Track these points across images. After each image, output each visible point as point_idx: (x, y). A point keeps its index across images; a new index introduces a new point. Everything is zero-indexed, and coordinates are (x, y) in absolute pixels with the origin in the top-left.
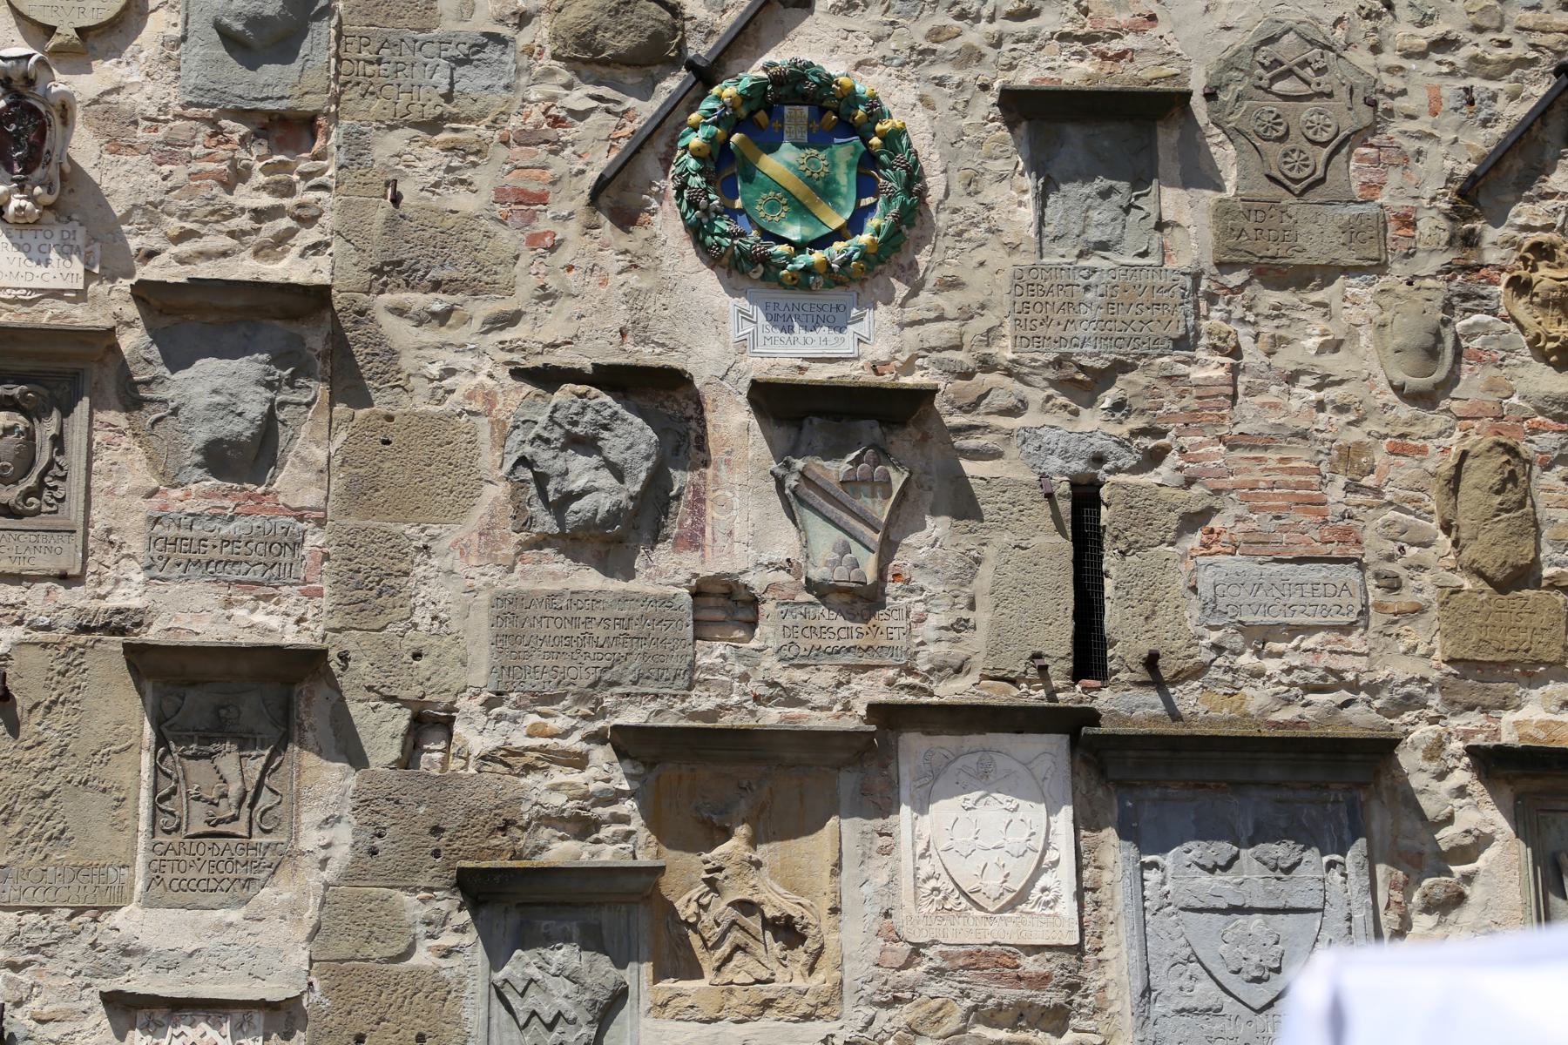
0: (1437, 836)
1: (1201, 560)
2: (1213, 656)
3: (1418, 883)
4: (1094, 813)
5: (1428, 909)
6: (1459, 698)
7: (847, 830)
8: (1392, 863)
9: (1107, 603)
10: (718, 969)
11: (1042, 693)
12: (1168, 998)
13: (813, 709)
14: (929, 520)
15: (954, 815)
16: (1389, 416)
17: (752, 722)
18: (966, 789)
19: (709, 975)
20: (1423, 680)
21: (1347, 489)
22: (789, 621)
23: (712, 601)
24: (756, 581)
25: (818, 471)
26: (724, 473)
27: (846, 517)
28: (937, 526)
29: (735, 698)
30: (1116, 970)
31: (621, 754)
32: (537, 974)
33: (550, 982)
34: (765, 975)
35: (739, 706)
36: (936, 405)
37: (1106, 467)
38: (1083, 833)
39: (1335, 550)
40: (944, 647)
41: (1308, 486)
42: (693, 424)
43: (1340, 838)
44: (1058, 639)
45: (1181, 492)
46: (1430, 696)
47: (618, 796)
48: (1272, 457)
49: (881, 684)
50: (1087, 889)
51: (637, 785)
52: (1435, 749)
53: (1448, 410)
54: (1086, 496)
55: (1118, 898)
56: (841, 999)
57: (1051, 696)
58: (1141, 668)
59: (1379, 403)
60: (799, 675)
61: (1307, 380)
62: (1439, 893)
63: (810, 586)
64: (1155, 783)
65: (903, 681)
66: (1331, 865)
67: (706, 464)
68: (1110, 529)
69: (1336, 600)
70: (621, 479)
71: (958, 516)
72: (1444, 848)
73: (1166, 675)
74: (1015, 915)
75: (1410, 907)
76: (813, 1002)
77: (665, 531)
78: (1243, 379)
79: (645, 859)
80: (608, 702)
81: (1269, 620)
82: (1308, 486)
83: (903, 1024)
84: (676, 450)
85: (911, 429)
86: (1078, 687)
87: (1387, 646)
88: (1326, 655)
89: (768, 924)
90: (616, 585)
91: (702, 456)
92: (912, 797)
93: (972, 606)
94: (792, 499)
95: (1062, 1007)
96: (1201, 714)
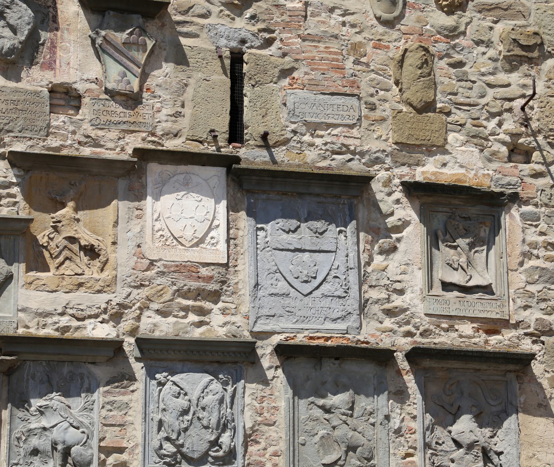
0: (386, 221)
1: (288, 91)
2: (292, 135)
3: (377, 241)
4: (236, 204)
5: (381, 253)
6: (399, 160)
7: (121, 207)
8: (367, 232)
9: (245, 109)
10: (57, 268)
11: (214, 148)
12: (266, 289)
13: (107, 149)
14: (164, 64)
15: (172, 202)
16: (374, 31)
17: (77, 154)
18: (178, 190)
19: (53, 270)
20: (384, 151)
21: (354, 63)
22: (96, 107)
23: (58, 96)
24: (81, 87)
25: (112, 37)
26: (66, 34)
27: (125, 60)
28: (168, 68)
29: (69, 142)
31: (13, 165)
34: (80, 271)
35: (71, 146)
36: (169, 10)
37: (246, 45)
38: (231, 213)
39: (348, 90)
40: (169, 124)
41: (337, 60)
42: (51, 10)
43: (345, 220)
44: (222, 124)
45: (280, 59)
46: (387, 158)
47: (10, 185)
48: (322, 46)
49: (140, 139)
50: (231, 238)
51: (20, 180)
52: (388, 182)
53: (399, 30)
54: (237, 58)
55: (246, 243)
56: (116, 284)
57: (218, 149)
58: (259, 139)
59: (369, 24)
60: (100, 133)
61: (338, 12)
62: (386, 246)
63: (107, 91)
64: (264, 192)
65: (150, 139)
66: (340, 232)
67: (57, 29)
68: (247, 74)
69: (347, 113)
70: (15, 34)
71: (178, 63)
73: (271, 143)
74: (198, 249)
75: (373, 252)
76: (103, 285)
77: (36, 60)
78: (310, 9)
79: (23, 215)
80: (7, 140)
81: (318, 120)
82: (337, 60)
83: (144, 296)
84: (43, 22)
85: (156, 21)
86: (231, 147)
87: (369, 135)
88: (342, 138)
89: (82, 248)
90: (12, 84)
91: (55, 25)
92: (152, 192)
93: (183, 106)
94: (99, 49)
95: (218, 291)
96: (286, 162)
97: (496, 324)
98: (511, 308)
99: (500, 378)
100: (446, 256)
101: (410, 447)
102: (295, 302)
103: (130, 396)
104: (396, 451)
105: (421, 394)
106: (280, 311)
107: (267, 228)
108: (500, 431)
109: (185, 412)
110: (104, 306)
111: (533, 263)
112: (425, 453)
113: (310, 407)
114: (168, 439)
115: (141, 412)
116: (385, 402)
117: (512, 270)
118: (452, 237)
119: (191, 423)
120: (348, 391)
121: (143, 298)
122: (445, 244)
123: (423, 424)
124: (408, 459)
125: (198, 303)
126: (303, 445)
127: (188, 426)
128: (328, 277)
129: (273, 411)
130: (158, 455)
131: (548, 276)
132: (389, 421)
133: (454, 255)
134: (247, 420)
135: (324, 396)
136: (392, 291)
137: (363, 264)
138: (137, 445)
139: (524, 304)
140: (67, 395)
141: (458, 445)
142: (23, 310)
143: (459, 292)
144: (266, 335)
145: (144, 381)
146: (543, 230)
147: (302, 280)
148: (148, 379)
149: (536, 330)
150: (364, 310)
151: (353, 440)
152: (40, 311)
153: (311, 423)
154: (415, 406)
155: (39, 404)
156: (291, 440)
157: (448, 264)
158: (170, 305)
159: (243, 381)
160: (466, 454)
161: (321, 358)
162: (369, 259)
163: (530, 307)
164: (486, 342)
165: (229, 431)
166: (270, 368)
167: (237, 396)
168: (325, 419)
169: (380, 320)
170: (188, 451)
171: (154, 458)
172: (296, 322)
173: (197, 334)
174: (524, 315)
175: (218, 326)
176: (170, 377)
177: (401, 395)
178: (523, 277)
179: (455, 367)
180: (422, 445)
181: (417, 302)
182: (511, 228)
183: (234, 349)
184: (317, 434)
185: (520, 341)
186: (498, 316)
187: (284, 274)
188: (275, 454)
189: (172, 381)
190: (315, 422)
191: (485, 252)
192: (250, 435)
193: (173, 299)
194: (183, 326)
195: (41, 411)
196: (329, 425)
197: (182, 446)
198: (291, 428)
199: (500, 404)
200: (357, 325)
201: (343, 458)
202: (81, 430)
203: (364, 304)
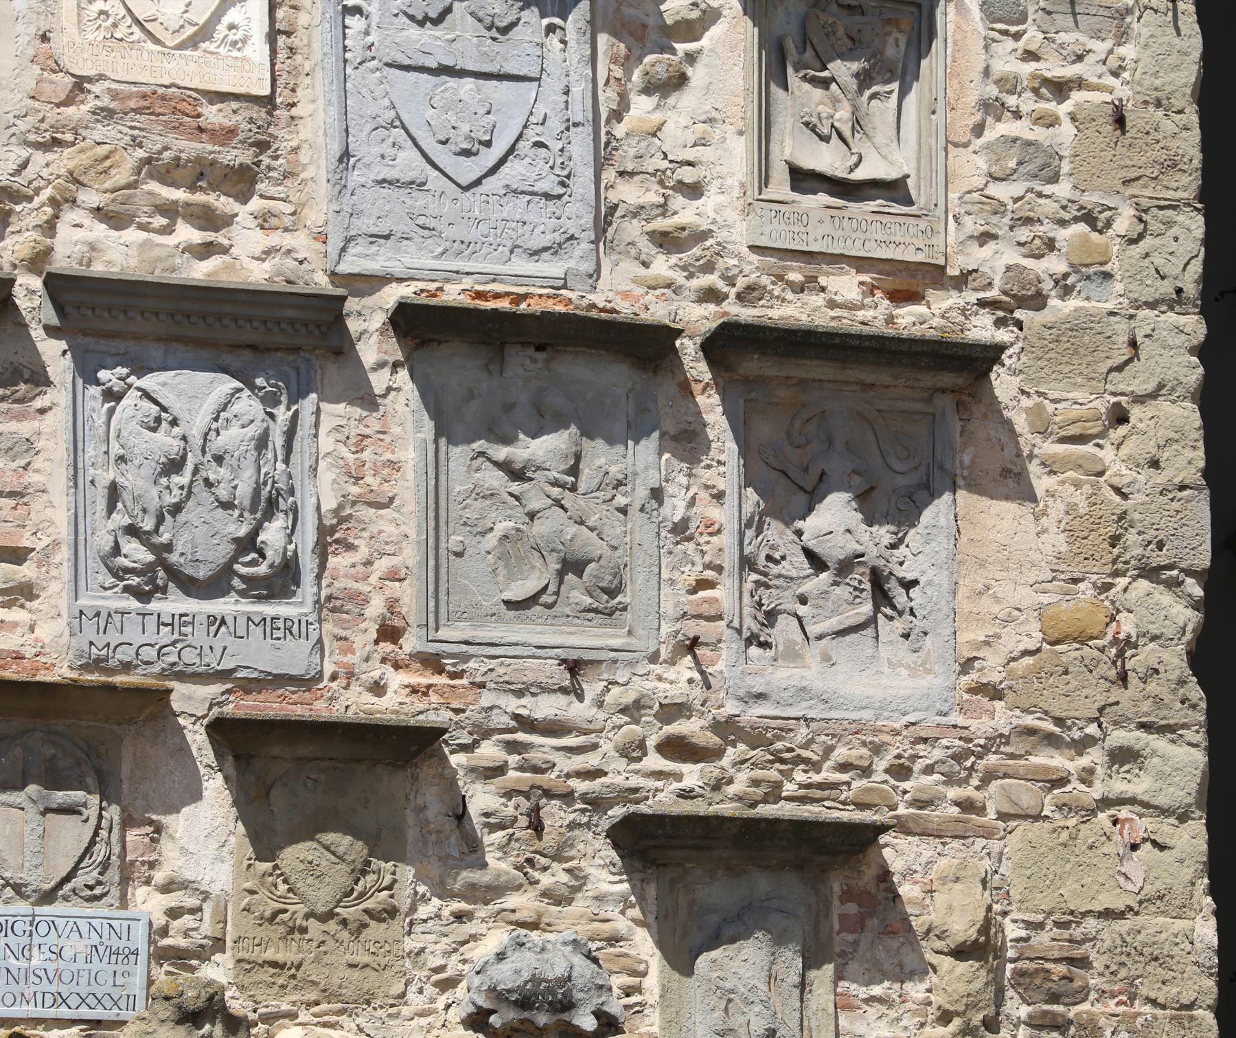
12: (368, 166)
30: (311, 129)
62: (661, 73)
72: (669, 22)
74: (197, 53)
75: (629, 86)
83: (63, 171)
97: (914, 276)
99: (919, 406)
100: (803, 105)
101: (708, 566)
102: (439, 202)
103: (37, 424)
104: (676, 574)
106: (402, 226)
107: (370, 9)
108: (912, 532)
109: (174, 466)
111: (1008, 127)
112: (742, 580)
113: (476, 463)
114: (132, 531)
115: (65, 463)
116: (652, 458)
117: (956, 145)
118: (818, 56)
119: (190, 493)
120: (567, 428)
121: (59, 177)
122: (801, 74)
123: (740, 512)
124: (702, 594)
125: (199, 197)
126: (460, 555)
127: (181, 501)
128: (521, 144)
129: (386, 471)
130: (110, 570)
131: (1039, 161)
132: (661, 503)
133: (822, 103)
134: (323, 491)
135: (508, 440)
136: (672, 188)
137: (604, 116)
138: (56, 544)
139: (982, 229)
141: (816, 562)
143: (832, 195)
144: (370, 283)
145: (69, 386)
146: (1033, 47)
147: (458, 150)
148: (80, 382)
149: (1005, 293)
150: (605, 231)
151: (577, 545)
153: (479, 504)
154: (722, 469)
156: (431, 541)
157: (807, 124)
158: (130, 196)
159: (313, 396)
160: (836, 583)
161: (503, 344)
162: (619, 104)
163: (994, 237)
164: (890, 320)
165: (282, 515)
166: (380, 365)
167: (299, 433)
168: (511, 494)
169: (643, 257)
170: (182, 560)
171: (100, 577)
172: (443, 253)
173: (200, 272)
174: (977, 256)
175: (251, 255)
176: (132, 379)
177: (688, 442)
178: (981, 162)
179: (817, 377)
180: (737, 561)
181: (732, 215)
182: (959, 37)
183: (290, 313)
184: (492, 529)
185: (967, 318)
186: (920, 257)
187: (413, 131)
189: (139, 389)
190: (488, 502)
191: (895, 96)
192: (333, 530)
193: (136, 181)
194: (162, 253)
196: (520, 509)
197: (169, 547)
198: (431, 514)
199: (916, 468)
200: (588, 266)
203: (606, 216)
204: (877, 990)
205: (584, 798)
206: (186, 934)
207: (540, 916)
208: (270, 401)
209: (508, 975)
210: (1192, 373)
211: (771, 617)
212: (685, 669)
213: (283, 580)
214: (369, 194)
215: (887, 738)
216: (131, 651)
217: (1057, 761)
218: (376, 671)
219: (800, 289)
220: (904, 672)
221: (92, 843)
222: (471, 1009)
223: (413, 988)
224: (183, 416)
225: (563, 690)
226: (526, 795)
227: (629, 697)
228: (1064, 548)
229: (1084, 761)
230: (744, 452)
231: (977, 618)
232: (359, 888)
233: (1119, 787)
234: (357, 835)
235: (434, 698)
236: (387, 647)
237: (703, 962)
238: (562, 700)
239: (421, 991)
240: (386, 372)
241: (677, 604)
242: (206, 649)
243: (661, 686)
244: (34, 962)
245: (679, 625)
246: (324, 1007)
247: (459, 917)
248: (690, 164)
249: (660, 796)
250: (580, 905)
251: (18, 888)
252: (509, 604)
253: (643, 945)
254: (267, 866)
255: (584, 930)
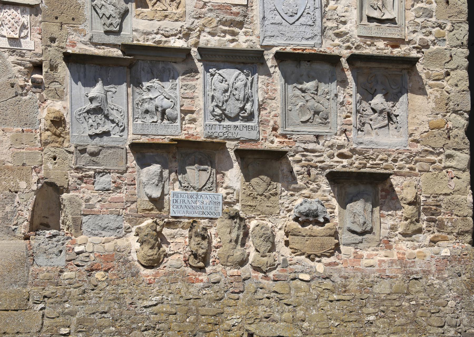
12: (269, 20)
32: (104, 4)
33: (108, 6)
83: (201, 24)
98: (406, 32)
99: (399, 73)
101: (348, 112)
102: (285, 28)
104: (341, 114)
105: (355, 82)
109: (226, 91)
110: (179, 29)
112: (356, 116)
114: (217, 106)
116: (335, 87)
117: (407, 10)
124: (347, 119)
125: (231, 29)
126: (290, 111)
131: (428, 13)
132: (337, 98)
134: (259, 96)
135: (301, 83)
137: (323, 6)
138: (201, 109)
140: (162, 80)
141: (374, 111)
142: (136, 31)
144: (269, 47)
148: (205, 72)
149: (419, 45)
151: (318, 108)
152: (145, 31)
155: (147, 85)
157: (371, 6)
160: (379, 116)
161: (300, 61)
163: (417, 31)
164: (392, 52)
166: (272, 66)
173: (231, 46)
174: (413, 36)
175: (243, 42)
176: (217, 71)
177: (343, 83)
178: (413, 14)
181: (353, 28)
183: (251, 55)
186: (399, 37)
188: (275, 116)
192: (262, 105)
195: (149, 89)
197: (225, 110)
198: (284, 101)
200: (320, 42)
201: (312, 118)
202: (170, 100)
204: (390, 213)
205: (320, 167)
206: (230, 199)
207: (310, 195)
208: (247, 75)
209: (303, 209)
210: (466, 63)
211: (364, 124)
212: (343, 137)
213: (250, 117)
214: (269, 26)
215: (392, 153)
216: (217, 134)
217: (433, 158)
218: (272, 138)
219: (370, 45)
220: (396, 137)
221: (210, 178)
222: (295, 217)
223: (281, 212)
224: (228, 79)
225: (315, 142)
226: (307, 167)
227: (330, 144)
228: (434, 106)
229: (440, 158)
230: (357, 85)
231: (413, 124)
232: (269, 188)
233: (448, 164)
234: (268, 176)
235: (285, 144)
236: (274, 132)
237: (348, 206)
238: (315, 144)
239: (283, 212)
240: (273, 68)
241: (341, 121)
242: (234, 133)
243: (338, 141)
244: (198, 204)
245: (342, 127)
246: (261, 216)
247: (292, 195)
248: (344, 16)
249: (338, 167)
250: (319, 193)
251: (194, 188)
252: (302, 122)
253: (334, 202)
254: (248, 183)
255: (320, 198)
